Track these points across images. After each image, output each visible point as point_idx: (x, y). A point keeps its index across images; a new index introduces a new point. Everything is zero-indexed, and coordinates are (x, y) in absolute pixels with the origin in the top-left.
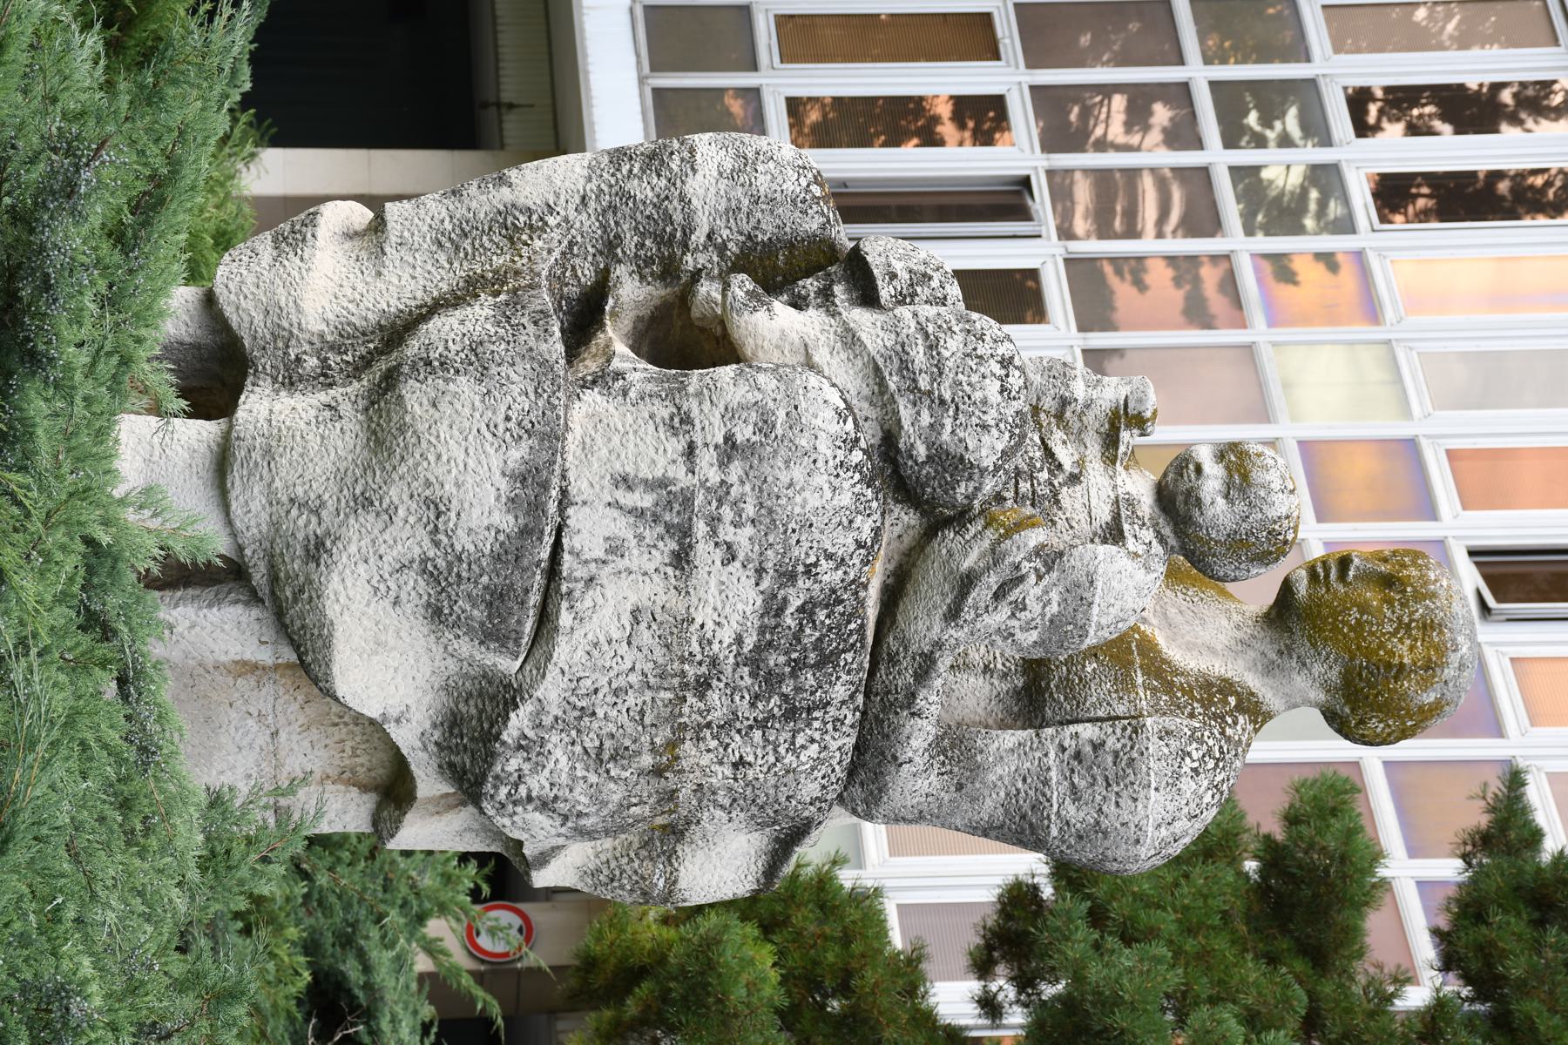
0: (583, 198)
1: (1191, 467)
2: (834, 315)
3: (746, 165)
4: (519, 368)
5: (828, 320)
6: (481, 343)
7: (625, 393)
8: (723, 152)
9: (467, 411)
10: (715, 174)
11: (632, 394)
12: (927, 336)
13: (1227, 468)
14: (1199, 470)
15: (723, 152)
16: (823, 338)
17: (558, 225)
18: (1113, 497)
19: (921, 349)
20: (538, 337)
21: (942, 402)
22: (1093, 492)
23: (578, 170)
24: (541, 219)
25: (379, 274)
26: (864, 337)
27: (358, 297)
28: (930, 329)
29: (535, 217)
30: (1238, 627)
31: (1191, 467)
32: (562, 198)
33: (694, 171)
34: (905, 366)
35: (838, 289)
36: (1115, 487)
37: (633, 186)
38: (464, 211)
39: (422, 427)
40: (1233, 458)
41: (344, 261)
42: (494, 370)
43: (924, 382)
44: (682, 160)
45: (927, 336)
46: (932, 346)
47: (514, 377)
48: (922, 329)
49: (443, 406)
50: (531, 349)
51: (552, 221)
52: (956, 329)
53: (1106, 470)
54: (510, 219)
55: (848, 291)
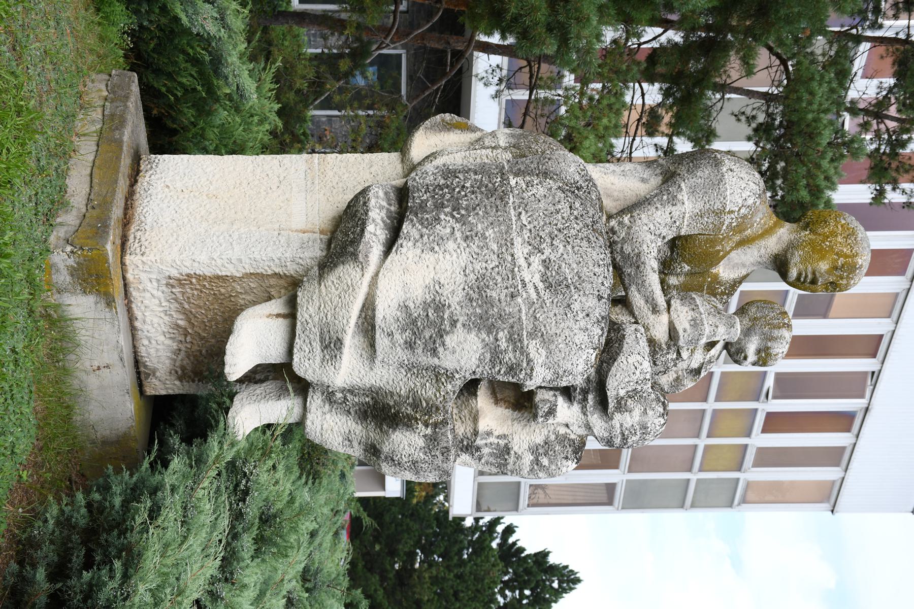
1: (743, 355)
2: (585, 414)
3: (557, 378)
5: (581, 416)
7: (480, 460)
10: (541, 381)
11: (483, 461)
13: (759, 359)
14: (745, 358)
16: (576, 423)
17: (460, 378)
18: (702, 361)
20: (443, 462)
22: (693, 361)
23: (473, 360)
27: (361, 376)
28: (626, 434)
30: (761, 257)
31: (743, 355)
32: (464, 369)
33: (531, 379)
35: (590, 397)
40: (763, 355)
42: (422, 473)
44: (526, 374)
51: (457, 376)
52: (638, 433)
55: (595, 397)
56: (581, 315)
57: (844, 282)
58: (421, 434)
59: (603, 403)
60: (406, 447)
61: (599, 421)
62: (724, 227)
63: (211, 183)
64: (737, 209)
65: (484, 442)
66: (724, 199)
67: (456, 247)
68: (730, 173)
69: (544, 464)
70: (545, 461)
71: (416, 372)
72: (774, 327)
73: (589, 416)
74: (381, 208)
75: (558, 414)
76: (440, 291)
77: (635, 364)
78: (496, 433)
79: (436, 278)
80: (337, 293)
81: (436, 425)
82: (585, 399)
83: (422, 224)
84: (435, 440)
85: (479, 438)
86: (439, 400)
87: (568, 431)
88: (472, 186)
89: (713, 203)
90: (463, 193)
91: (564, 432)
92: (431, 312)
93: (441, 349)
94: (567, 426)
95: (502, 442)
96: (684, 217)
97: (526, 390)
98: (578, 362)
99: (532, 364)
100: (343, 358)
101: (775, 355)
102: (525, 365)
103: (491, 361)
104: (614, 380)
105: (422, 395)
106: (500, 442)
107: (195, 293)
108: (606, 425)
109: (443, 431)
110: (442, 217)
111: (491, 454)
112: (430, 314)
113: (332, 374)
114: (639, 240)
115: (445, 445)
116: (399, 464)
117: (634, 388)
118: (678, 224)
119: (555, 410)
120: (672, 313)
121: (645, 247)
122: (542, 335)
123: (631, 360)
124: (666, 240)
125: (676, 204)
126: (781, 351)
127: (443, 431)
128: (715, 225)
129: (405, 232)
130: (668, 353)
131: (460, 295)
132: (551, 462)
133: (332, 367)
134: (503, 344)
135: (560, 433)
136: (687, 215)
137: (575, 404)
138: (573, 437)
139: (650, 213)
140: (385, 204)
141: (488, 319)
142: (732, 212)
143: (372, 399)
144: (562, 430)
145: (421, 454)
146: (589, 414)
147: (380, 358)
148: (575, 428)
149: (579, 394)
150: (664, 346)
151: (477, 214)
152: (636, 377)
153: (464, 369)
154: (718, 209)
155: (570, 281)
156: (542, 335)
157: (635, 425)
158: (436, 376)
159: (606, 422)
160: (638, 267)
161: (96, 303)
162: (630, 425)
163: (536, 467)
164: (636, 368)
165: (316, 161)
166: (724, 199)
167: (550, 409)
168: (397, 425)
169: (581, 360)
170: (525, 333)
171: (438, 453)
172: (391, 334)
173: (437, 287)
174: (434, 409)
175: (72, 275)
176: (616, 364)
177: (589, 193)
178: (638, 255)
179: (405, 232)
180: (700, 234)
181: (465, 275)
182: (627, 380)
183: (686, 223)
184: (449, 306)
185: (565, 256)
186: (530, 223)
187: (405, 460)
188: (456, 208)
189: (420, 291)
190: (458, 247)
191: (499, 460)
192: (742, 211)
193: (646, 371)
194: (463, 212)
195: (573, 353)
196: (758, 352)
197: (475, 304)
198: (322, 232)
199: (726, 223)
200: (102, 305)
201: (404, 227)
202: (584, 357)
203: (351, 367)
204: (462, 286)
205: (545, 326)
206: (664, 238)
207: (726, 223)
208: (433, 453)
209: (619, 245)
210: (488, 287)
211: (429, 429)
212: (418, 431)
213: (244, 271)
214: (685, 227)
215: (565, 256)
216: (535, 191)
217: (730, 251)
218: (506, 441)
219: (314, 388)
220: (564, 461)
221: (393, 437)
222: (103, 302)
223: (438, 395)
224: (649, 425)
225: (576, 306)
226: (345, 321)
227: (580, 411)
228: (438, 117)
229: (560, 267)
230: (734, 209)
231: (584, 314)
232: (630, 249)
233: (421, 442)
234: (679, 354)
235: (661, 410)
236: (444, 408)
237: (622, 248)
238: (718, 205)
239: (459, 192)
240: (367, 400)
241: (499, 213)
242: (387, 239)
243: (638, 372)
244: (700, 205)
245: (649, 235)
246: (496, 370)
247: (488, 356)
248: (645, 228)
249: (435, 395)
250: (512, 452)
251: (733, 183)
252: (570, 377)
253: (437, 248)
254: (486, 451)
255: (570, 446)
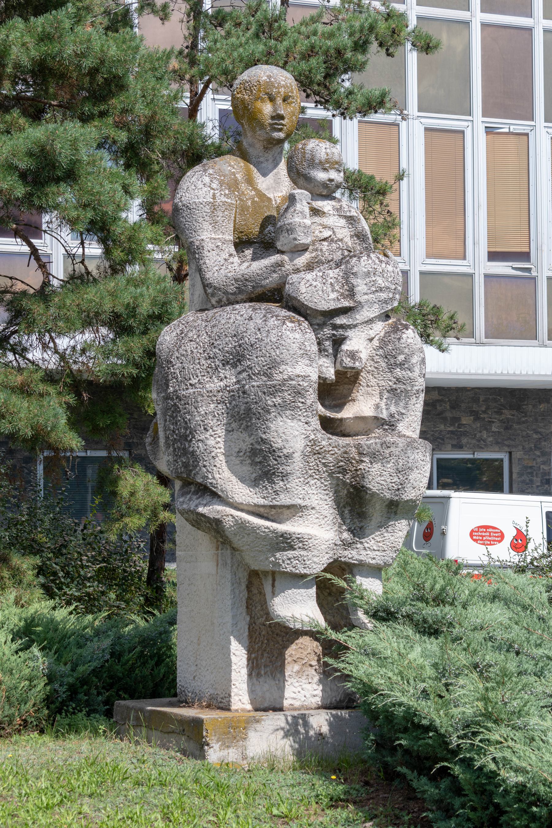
0: (306, 423)
2: (355, 326)
4: (410, 455)
6: (397, 469)
7: (403, 414)
8: (300, 363)
9: (419, 475)
10: (310, 368)
11: (404, 411)
12: (377, 291)
13: (331, 169)
14: (331, 180)
15: (300, 363)
16: (366, 332)
17: (315, 434)
19: (381, 294)
21: (395, 289)
22: (337, 224)
23: (292, 424)
24: (310, 441)
25: (313, 508)
26: (372, 316)
27: (322, 517)
28: (374, 289)
29: (309, 444)
32: (304, 432)
34: (386, 302)
36: (334, 215)
37: (309, 402)
38: (298, 472)
39: (419, 493)
41: (300, 522)
42: (410, 465)
43: (391, 295)
44: (303, 381)
45: (377, 291)
46: (381, 290)
47: (413, 457)
48: (374, 292)
49: (415, 484)
50: (402, 450)
51: (312, 437)
52: (374, 279)
53: (326, 217)
54: (307, 454)
56: (259, 336)
57: (282, 90)
58: (370, 466)
59: (345, 311)
60: (382, 478)
61: (362, 313)
62: (229, 201)
63: (192, 642)
64: (212, 191)
65: (384, 411)
66: (201, 204)
67: (212, 438)
68: (183, 199)
69: (403, 359)
70: (401, 358)
71: (312, 471)
72: (304, 157)
73: (358, 322)
74: (190, 500)
75: (356, 348)
76: (244, 452)
77: (307, 285)
78: (378, 400)
79: (235, 455)
80: (246, 536)
81: (360, 454)
82: (342, 327)
83: (196, 466)
84: (375, 454)
85: (381, 416)
86: (337, 452)
87: (377, 338)
88: (173, 424)
89: (205, 214)
90: (177, 432)
91: (378, 342)
92: (257, 460)
93: (285, 452)
94: (371, 340)
95: (386, 395)
96: (214, 239)
97: (333, 377)
98: (292, 338)
99: (292, 377)
100: (300, 532)
101: (328, 155)
102: (294, 382)
103: (293, 410)
104: (320, 303)
105: (333, 466)
106: (385, 397)
107: (266, 655)
108: (366, 307)
109: (366, 447)
110: (191, 449)
111: (397, 404)
112: (258, 460)
113: (317, 542)
114: (224, 279)
115: (379, 445)
116: (401, 484)
117: (329, 286)
118: (220, 244)
119: (351, 352)
120: (284, 250)
121: (229, 275)
122: (270, 368)
123: (303, 289)
124: (235, 253)
125: (203, 247)
126: (324, 151)
127: (366, 447)
128: (226, 209)
129: (202, 480)
130: (321, 250)
131: (245, 435)
132: (402, 353)
133: (310, 541)
134: (278, 400)
135: (378, 345)
136: (213, 236)
137: (346, 334)
138: (382, 334)
139: (206, 270)
140: (188, 496)
141: (259, 413)
142: (214, 197)
143: (345, 507)
144: (376, 343)
145: (389, 466)
146: (355, 323)
147: (300, 502)
148: (372, 333)
149: (337, 331)
150: (313, 255)
151: (189, 420)
152: (319, 284)
153: (304, 432)
154: (211, 208)
155: (237, 344)
156: (270, 368)
157: (365, 282)
158: (315, 454)
159: (363, 307)
160: (246, 280)
161: (256, 730)
162: (365, 287)
163: (406, 366)
164: (311, 285)
165: (180, 553)
166: (201, 204)
167: (349, 356)
168: (363, 487)
169: (291, 336)
170: (268, 383)
171: (387, 451)
172: (276, 493)
173: (241, 454)
174: (346, 456)
175: (228, 747)
176: (305, 303)
177: (188, 323)
178: (236, 280)
179: (202, 480)
180: (235, 221)
181: (233, 430)
182: (320, 293)
183: (220, 236)
184: (252, 444)
185: (220, 347)
186: (197, 376)
187: (396, 479)
188: (185, 437)
189: (244, 468)
190: (212, 436)
191: (402, 398)
192: (214, 186)
193: (315, 277)
194: (188, 432)
195: (283, 343)
196: (325, 170)
197: (249, 424)
198: (217, 549)
199: (224, 199)
200: (258, 726)
201: (199, 481)
202: (288, 333)
203: (312, 525)
204: (240, 433)
205: (264, 366)
206: (231, 255)
207: (224, 199)
208: (388, 455)
209: (230, 296)
210: (239, 412)
211: (364, 459)
212: (367, 469)
213: (244, 614)
214: (224, 237)
215: (220, 347)
216: (178, 371)
217: (255, 189)
218: (385, 391)
219: (340, 557)
220: (402, 341)
221: (374, 490)
222: (255, 725)
223: (332, 452)
224: (366, 270)
225: (253, 340)
226: (266, 530)
227: (353, 330)
228: (148, 448)
229: (227, 352)
230: (211, 194)
231: (258, 333)
232: (232, 287)
233: (377, 466)
234: (325, 240)
235: (355, 259)
236: (345, 447)
237: (232, 294)
238: (207, 209)
239: (176, 435)
240: (346, 512)
241: (190, 402)
242: (210, 495)
243: (314, 284)
244: (206, 225)
245: (222, 271)
246: (301, 405)
247: (288, 412)
248: (215, 275)
249: (332, 454)
250: (394, 386)
251: (190, 196)
252: (306, 343)
253: (213, 454)
254: (393, 409)
255: (390, 336)
